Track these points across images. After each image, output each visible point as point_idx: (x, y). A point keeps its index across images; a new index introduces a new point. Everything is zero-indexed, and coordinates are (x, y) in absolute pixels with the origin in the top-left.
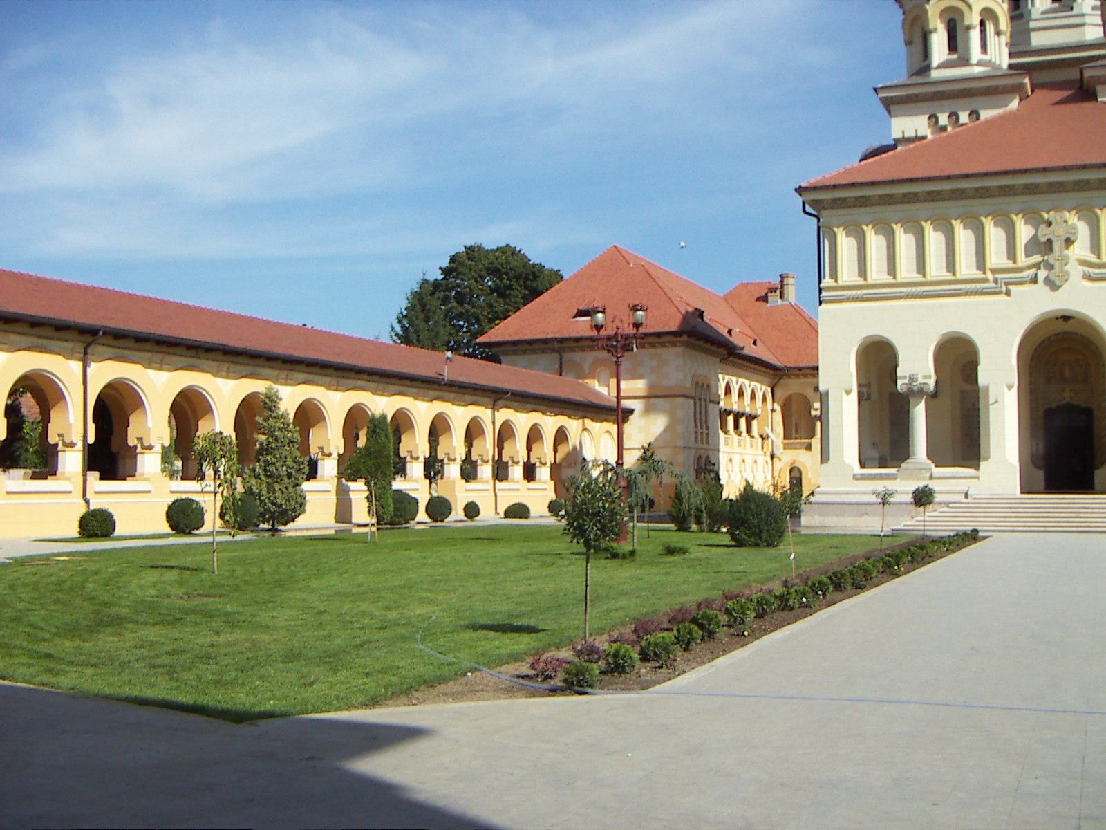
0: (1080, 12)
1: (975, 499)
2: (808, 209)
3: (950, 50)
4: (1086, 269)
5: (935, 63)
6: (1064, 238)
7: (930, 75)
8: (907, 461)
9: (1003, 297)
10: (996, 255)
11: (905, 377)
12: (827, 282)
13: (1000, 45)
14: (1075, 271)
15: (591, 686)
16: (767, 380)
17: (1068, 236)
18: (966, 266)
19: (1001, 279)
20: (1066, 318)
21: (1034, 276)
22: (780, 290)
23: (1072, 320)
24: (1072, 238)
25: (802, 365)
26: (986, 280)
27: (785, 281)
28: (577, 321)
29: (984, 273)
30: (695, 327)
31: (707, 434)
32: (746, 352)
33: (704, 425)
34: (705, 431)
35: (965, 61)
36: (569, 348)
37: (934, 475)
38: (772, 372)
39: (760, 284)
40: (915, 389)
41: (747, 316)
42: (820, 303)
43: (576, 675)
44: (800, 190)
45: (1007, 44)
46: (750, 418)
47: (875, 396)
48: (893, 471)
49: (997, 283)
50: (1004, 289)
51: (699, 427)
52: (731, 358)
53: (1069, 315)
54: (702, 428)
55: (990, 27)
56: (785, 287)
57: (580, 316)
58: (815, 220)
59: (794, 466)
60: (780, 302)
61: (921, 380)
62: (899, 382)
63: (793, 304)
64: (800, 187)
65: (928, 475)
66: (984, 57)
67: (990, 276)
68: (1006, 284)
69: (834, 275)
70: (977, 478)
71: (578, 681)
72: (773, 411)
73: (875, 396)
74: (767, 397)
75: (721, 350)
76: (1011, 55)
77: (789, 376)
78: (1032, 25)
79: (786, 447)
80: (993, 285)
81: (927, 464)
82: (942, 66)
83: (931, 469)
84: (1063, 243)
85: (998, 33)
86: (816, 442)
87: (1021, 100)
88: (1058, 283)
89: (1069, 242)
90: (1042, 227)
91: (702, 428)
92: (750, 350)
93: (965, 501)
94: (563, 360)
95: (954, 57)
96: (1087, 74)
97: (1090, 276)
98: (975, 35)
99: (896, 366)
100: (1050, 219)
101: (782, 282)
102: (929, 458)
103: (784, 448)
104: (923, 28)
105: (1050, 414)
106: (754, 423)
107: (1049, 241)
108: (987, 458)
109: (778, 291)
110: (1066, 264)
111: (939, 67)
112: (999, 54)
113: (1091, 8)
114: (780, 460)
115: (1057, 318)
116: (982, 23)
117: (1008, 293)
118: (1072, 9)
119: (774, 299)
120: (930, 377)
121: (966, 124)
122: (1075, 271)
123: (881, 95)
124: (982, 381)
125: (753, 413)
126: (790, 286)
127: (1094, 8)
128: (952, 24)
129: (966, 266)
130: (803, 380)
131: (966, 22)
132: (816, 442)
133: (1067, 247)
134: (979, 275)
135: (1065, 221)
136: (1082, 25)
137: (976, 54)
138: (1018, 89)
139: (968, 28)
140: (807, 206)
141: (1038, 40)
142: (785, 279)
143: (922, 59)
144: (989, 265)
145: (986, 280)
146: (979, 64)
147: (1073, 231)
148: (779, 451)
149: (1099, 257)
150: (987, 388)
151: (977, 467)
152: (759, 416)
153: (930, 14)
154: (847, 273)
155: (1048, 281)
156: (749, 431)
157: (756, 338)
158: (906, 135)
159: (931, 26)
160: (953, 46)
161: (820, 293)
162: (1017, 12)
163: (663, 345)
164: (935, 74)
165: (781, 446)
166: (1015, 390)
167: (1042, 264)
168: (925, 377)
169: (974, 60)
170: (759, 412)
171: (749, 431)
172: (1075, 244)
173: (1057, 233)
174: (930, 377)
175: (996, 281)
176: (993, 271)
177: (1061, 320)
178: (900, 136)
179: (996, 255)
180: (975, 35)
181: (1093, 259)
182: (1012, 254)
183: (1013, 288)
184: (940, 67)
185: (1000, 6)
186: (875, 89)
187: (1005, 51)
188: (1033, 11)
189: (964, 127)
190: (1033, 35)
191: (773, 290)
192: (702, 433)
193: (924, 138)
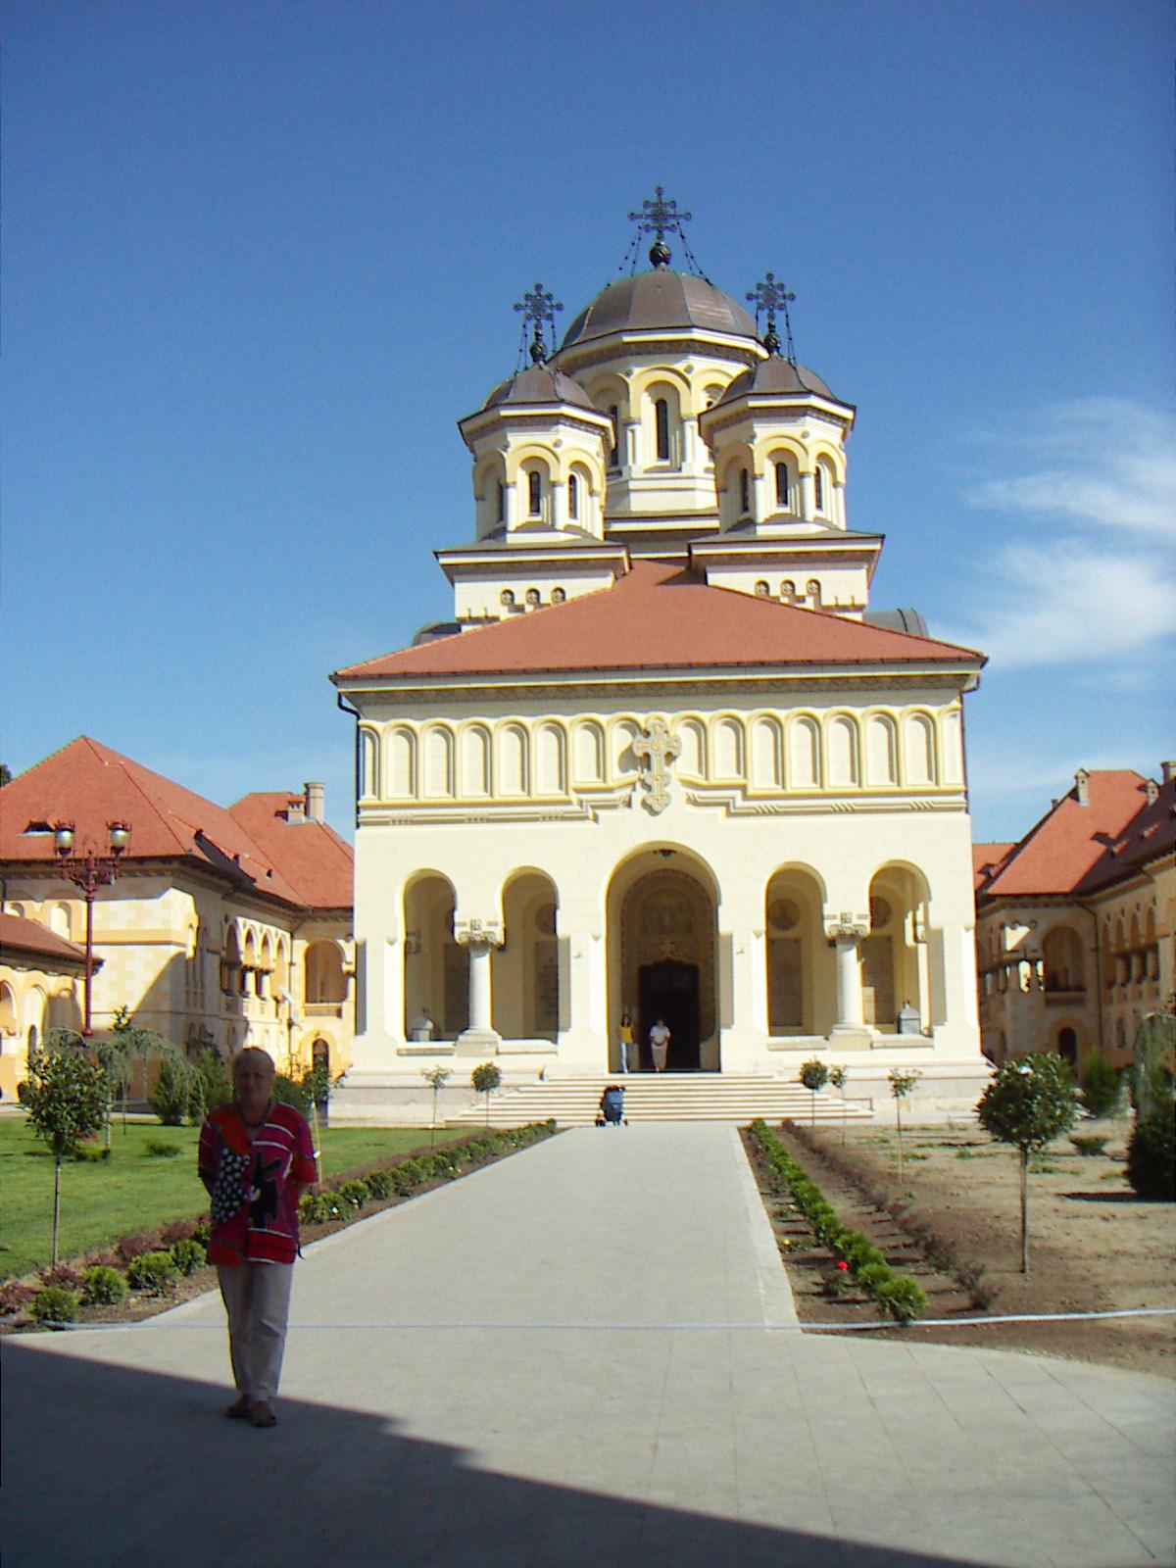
0: (690, 475)
1: (551, 1080)
2: (346, 703)
3: (532, 511)
4: (691, 792)
5: (512, 525)
6: (665, 752)
7: (505, 540)
8: (467, 1032)
9: (590, 824)
10: (582, 772)
11: (464, 924)
12: (368, 798)
13: (592, 508)
14: (678, 793)
15: (69, 1320)
16: (285, 923)
17: (670, 750)
18: (545, 784)
19: (588, 801)
20: (666, 852)
21: (627, 799)
22: (305, 803)
23: (673, 855)
24: (674, 753)
25: (331, 904)
26: (569, 803)
27: (312, 793)
28: (29, 838)
29: (567, 793)
30: (191, 850)
31: (202, 994)
32: (259, 885)
33: (199, 985)
34: (199, 991)
36: (15, 873)
37: (500, 1050)
38: (291, 913)
39: (278, 795)
40: (478, 939)
41: (261, 837)
42: (358, 825)
43: (52, 1306)
44: (336, 679)
45: (601, 507)
46: (260, 973)
47: (426, 949)
48: (448, 1045)
49: (581, 806)
50: (590, 813)
51: (192, 985)
52: (238, 894)
53: (671, 848)
54: (196, 985)
55: (582, 484)
56: (312, 800)
57: (33, 830)
58: (354, 717)
59: (319, 1037)
60: (303, 819)
61: (485, 928)
62: (457, 930)
63: (321, 823)
64: (336, 674)
65: (493, 1050)
66: (573, 522)
67: (574, 797)
68: (593, 807)
69: (377, 790)
70: (556, 1053)
71: (54, 1313)
72: (291, 964)
73: (426, 949)
74: (284, 944)
75: (224, 883)
76: (607, 520)
77: (314, 920)
79: (307, 1014)
80: (576, 808)
81: (489, 1036)
83: (496, 1042)
84: (663, 758)
86: (348, 1007)
87: (616, 578)
88: (656, 808)
89: (670, 757)
90: (640, 737)
91: (196, 985)
92: (263, 884)
93: (540, 1083)
94: (8, 890)
96: (695, 552)
97: (695, 801)
98: (562, 494)
99: (453, 909)
100: (648, 729)
101: (307, 794)
102: (494, 1027)
103: (306, 1015)
104: (499, 479)
105: (645, 972)
106: (266, 979)
107: (647, 755)
108: (567, 1029)
109: (302, 806)
110: (666, 785)
112: (592, 520)
113: (702, 471)
114: (301, 1030)
115: (655, 852)
116: (572, 480)
117: (596, 819)
119: (296, 816)
120: (496, 924)
121: (549, 605)
122: (678, 793)
123: (444, 560)
124: (562, 931)
125: (265, 967)
126: (318, 800)
127: (707, 470)
128: (535, 478)
129: (545, 784)
130: (332, 924)
131: (553, 478)
132: (348, 1007)
133: (668, 764)
134: (562, 796)
135: (666, 732)
136: (692, 489)
137: (563, 518)
138: (612, 565)
140: (344, 700)
141: (638, 503)
142: (312, 791)
143: (495, 520)
144: (572, 784)
145: (569, 803)
146: (568, 529)
147: (675, 744)
148: (299, 1018)
149: (707, 778)
150: (568, 941)
151: (555, 1041)
152: (273, 971)
153: (507, 463)
154: (394, 787)
155: (644, 804)
156: (258, 991)
157: (272, 867)
158: (474, 615)
159: (509, 479)
161: (358, 812)
162: (614, 469)
163: (147, 874)
164: (512, 539)
165: (302, 1012)
166: (602, 942)
167: (638, 785)
168: (490, 924)
169: (560, 525)
170: (273, 965)
171: (258, 991)
172: (678, 760)
173: (656, 747)
174: (496, 924)
175: (581, 803)
176: (578, 791)
177: (660, 855)
178: (465, 614)
179: (582, 772)
180: (562, 494)
181: (700, 780)
182: (601, 769)
183: (599, 812)
184: (519, 530)
185: (594, 460)
186: (436, 554)
187: (599, 516)
188: (634, 468)
189: (545, 609)
190: (633, 496)
191: (294, 803)
192: (195, 993)
193: (496, 619)
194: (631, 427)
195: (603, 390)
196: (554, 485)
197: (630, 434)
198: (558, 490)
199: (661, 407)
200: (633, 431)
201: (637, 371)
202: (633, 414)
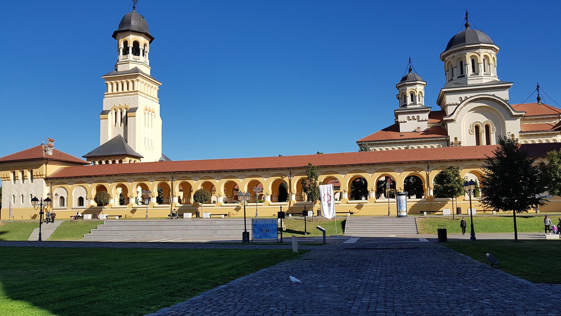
35: (415, 104)
78: (468, 79)
82: (410, 105)
85: (422, 97)
95: (412, 103)
98: (417, 98)
111: (410, 105)
118: (478, 74)
137: (418, 102)
139: (416, 96)
146: (419, 104)
159: (407, 96)
160: (412, 100)
162: (462, 75)
169: (417, 104)
178: (400, 121)
193: (406, 122)
194: (467, 66)
195: (458, 59)
196: (416, 96)
197: (466, 67)
198: (417, 97)
199: (473, 61)
200: (467, 67)
201: (468, 53)
202: (467, 63)
